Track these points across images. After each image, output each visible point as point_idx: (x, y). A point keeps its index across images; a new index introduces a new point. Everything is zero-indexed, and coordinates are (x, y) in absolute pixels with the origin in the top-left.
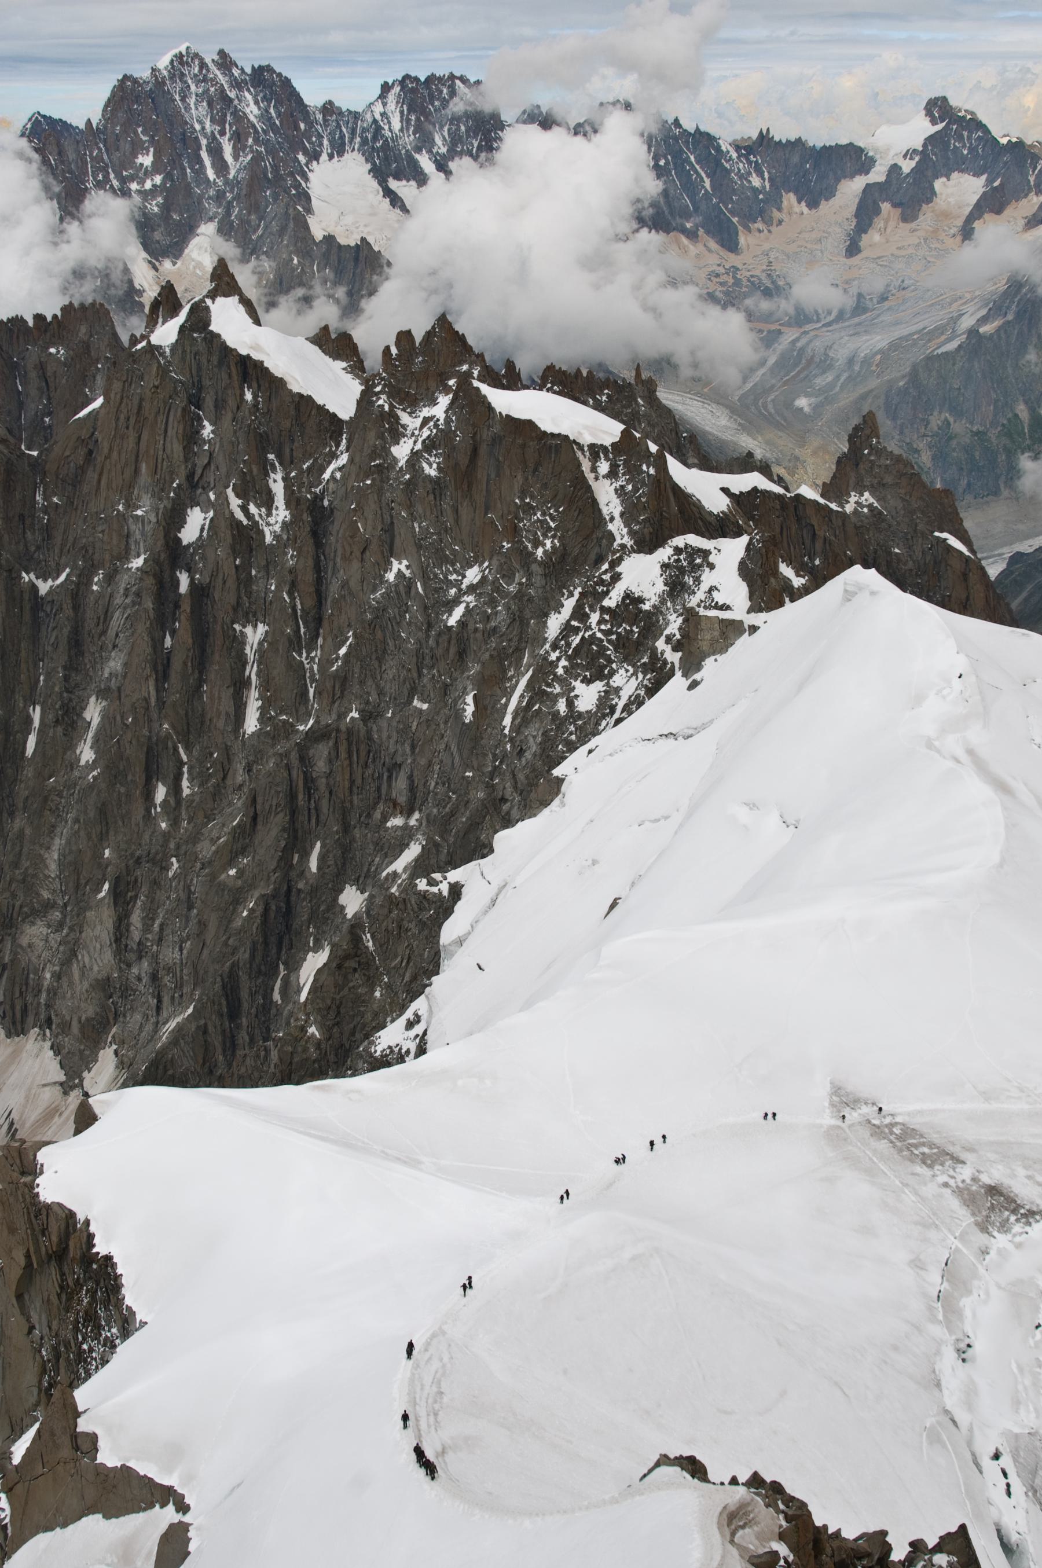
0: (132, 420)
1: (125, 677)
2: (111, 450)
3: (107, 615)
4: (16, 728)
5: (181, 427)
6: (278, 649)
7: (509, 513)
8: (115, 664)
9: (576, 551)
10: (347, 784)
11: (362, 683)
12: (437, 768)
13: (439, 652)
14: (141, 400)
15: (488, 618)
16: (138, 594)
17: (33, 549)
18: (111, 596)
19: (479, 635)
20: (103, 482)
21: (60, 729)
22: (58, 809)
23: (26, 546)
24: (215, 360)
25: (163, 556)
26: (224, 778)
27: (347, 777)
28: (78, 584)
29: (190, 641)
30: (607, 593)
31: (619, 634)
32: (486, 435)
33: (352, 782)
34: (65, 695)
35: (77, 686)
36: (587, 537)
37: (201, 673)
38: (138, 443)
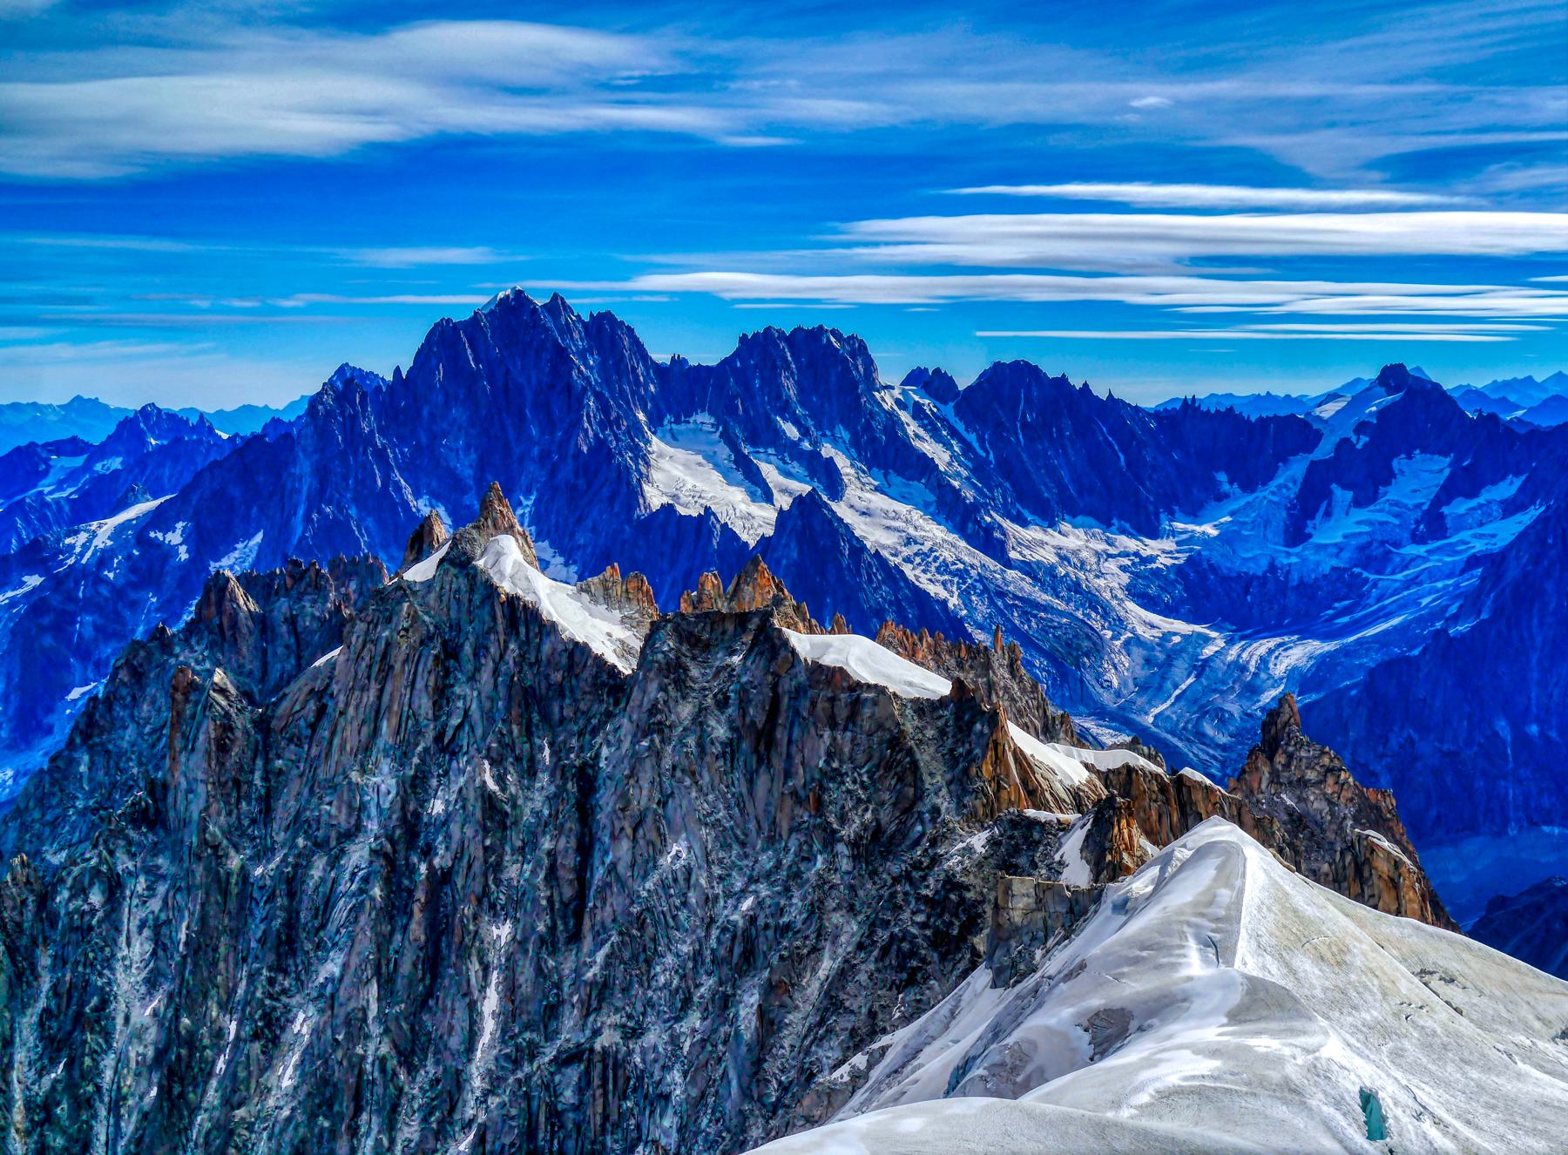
0: (376, 668)
1: (341, 979)
2: (347, 704)
3: (329, 903)
4: (206, 1042)
5: (432, 678)
6: (527, 951)
7: (813, 779)
8: (332, 967)
9: (893, 827)
10: (599, 1120)
11: (625, 990)
12: (711, 1100)
13: (722, 952)
14: (388, 644)
15: (781, 911)
16: (366, 880)
17: (246, 822)
18: (334, 881)
19: (770, 933)
20: (336, 741)
21: (257, 1047)
22: (245, 1146)
23: (239, 818)
24: (477, 599)
25: (398, 832)
26: (452, 1110)
27: (600, 1110)
28: (296, 866)
29: (423, 938)
30: (924, 878)
31: (937, 931)
32: (787, 685)
33: (606, 1117)
34: (267, 1002)
35: (284, 992)
36: (907, 811)
37: (434, 979)
38: (380, 697)
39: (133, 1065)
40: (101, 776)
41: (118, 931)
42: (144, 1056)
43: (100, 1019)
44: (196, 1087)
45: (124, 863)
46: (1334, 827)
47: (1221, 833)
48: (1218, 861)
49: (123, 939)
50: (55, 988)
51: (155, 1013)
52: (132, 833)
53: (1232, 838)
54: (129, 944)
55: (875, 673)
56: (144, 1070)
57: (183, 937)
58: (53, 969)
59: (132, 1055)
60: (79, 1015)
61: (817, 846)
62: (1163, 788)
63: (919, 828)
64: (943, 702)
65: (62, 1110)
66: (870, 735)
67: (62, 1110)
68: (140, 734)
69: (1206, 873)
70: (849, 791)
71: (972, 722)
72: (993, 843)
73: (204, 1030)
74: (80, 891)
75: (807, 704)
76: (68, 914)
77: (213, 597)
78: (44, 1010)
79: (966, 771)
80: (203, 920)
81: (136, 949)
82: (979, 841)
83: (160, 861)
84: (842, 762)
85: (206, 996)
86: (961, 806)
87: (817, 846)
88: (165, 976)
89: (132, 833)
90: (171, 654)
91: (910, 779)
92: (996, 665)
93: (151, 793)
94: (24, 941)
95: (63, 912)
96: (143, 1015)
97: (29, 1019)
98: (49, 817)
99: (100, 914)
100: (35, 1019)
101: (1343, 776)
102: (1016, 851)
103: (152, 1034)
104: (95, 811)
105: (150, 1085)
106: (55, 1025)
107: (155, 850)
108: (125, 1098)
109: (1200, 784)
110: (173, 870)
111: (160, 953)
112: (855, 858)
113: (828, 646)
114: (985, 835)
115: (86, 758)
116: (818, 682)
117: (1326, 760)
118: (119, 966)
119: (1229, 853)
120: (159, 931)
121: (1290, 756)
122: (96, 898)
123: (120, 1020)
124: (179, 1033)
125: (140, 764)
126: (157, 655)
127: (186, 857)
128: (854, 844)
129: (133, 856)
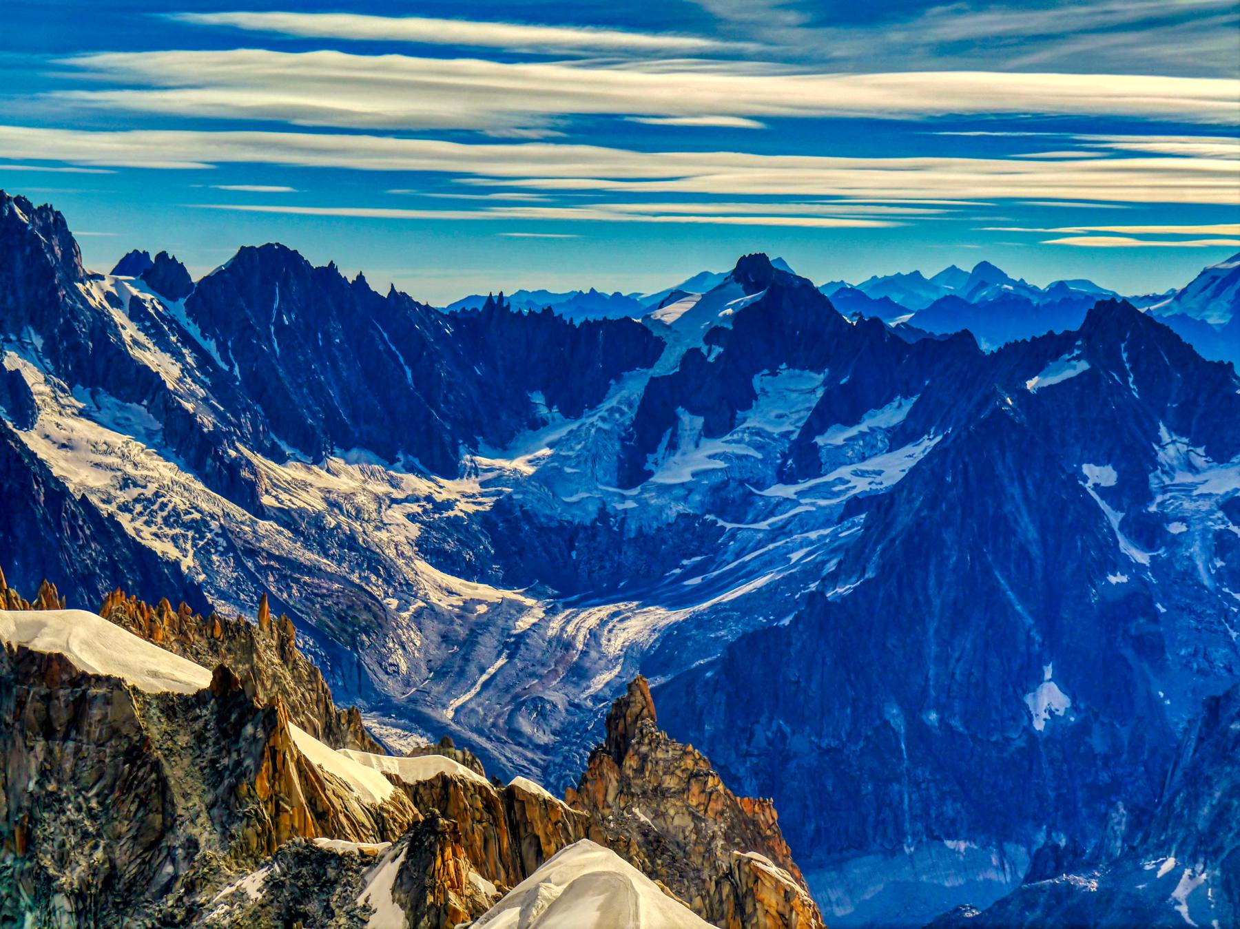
7: (20, 809)
9: (133, 869)
36: (153, 846)
46: (702, 849)
47: (594, 862)
48: (600, 899)
53: (610, 868)
55: (106, 661)
61: (25, 900)
62: (489, 805)
63: (169, 869)
64: (200, 698)
66: (100, 744)
69: (587, 911)
70: (71, 823)
71: (241, 724)
72: (273, 885)
75: (12, 705)
79: (233, 789)
82: (253, 884)
84: (59, 782)
86: (227, 836)
87: (25, 900)
91: (156, 803)
92: (261, 646)
101: (711, 782)
102: (305, 894)
109: (536, 797)
112: (78, 913)
113: (42, 625)
114: (261, 874)
116: (27, 675)
117: (689, 763)
119: (614, 887)
121: (644, 758)
128: (78, 896)
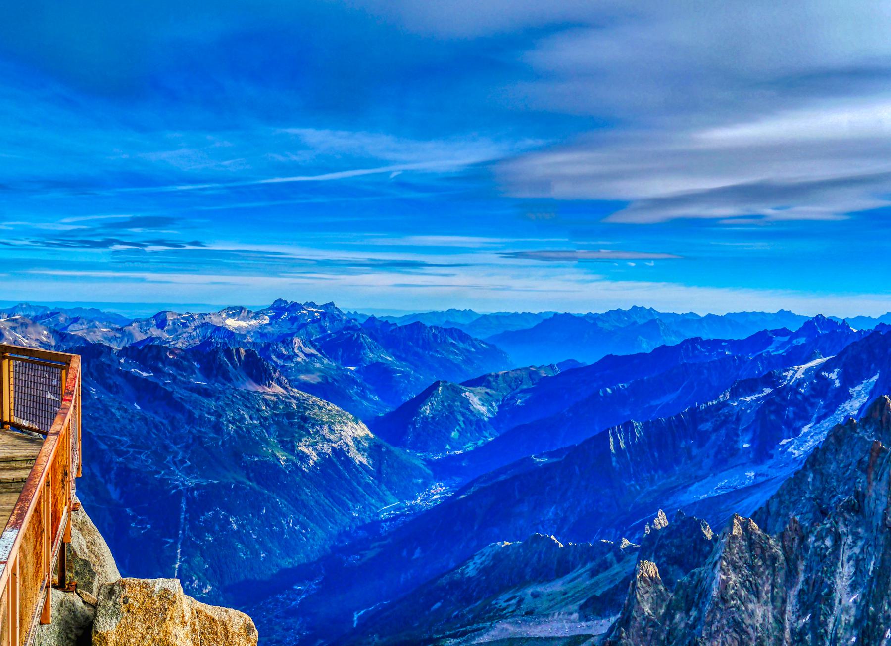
4: (881, 621)
39: (844, 624)
40: (818, 484)
41: (838, 559)
42: (849, 621)
43: (828, 599)
44: (875, 641)
45: (842, 529)
49: (840, 563)
50: (807, 581)
51: (855, 602)
52: (847, 516)
54: (843, 566)
56: (849, 628)
57: (872, 569)
58: (805, 571)
59: (843, 619)
60: (818, 595)
65: (808, 637)
67: (808, 637)
68: (838, 467)
73: (880, 615)
74: (820, 537)
76: (814, 547)
77: (878, 407)
78: (801, 590)
80: (883, 561)
81: (846, 570)
83: (860, 530)
85: (882, 599)
88: (860, 585)
89: (847, 516)
90: (856, 432)
93: (857, 497)
94: (793, 557)
95: (811, 546)
96: (850, 601)
97: (793, 593)
98: (792, 500)
99: (830, 550)
100: (796, 593)
103: (853, 611)
104: (814, 500)
105: (852, 636)
106: (806, 598)
107: (857, 524)
108: (839, 639)
110: (866, 535)
111: (858, 573)
115: (812, 475)
118: (837, 576)
120: (859, 563)
122: (828, 542)
123: (837, 602)
124: (868, 614)
125: (837, 481)
126: (849, 432)
127: (874, 531)
129: (847, 526)
